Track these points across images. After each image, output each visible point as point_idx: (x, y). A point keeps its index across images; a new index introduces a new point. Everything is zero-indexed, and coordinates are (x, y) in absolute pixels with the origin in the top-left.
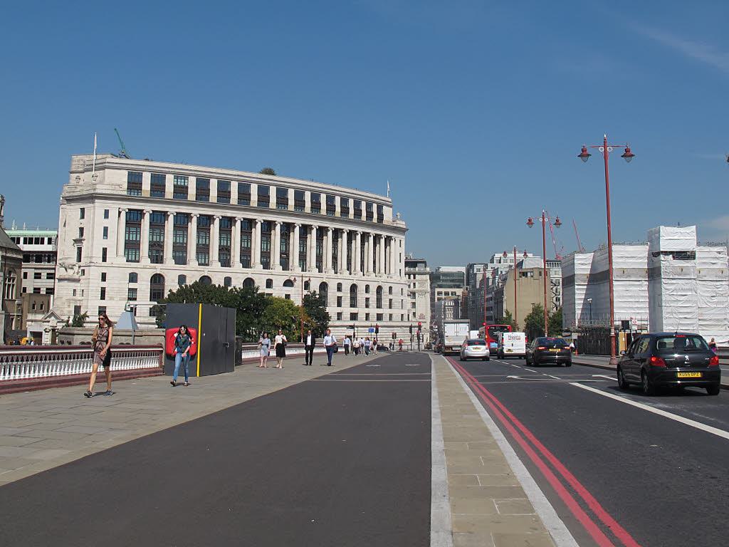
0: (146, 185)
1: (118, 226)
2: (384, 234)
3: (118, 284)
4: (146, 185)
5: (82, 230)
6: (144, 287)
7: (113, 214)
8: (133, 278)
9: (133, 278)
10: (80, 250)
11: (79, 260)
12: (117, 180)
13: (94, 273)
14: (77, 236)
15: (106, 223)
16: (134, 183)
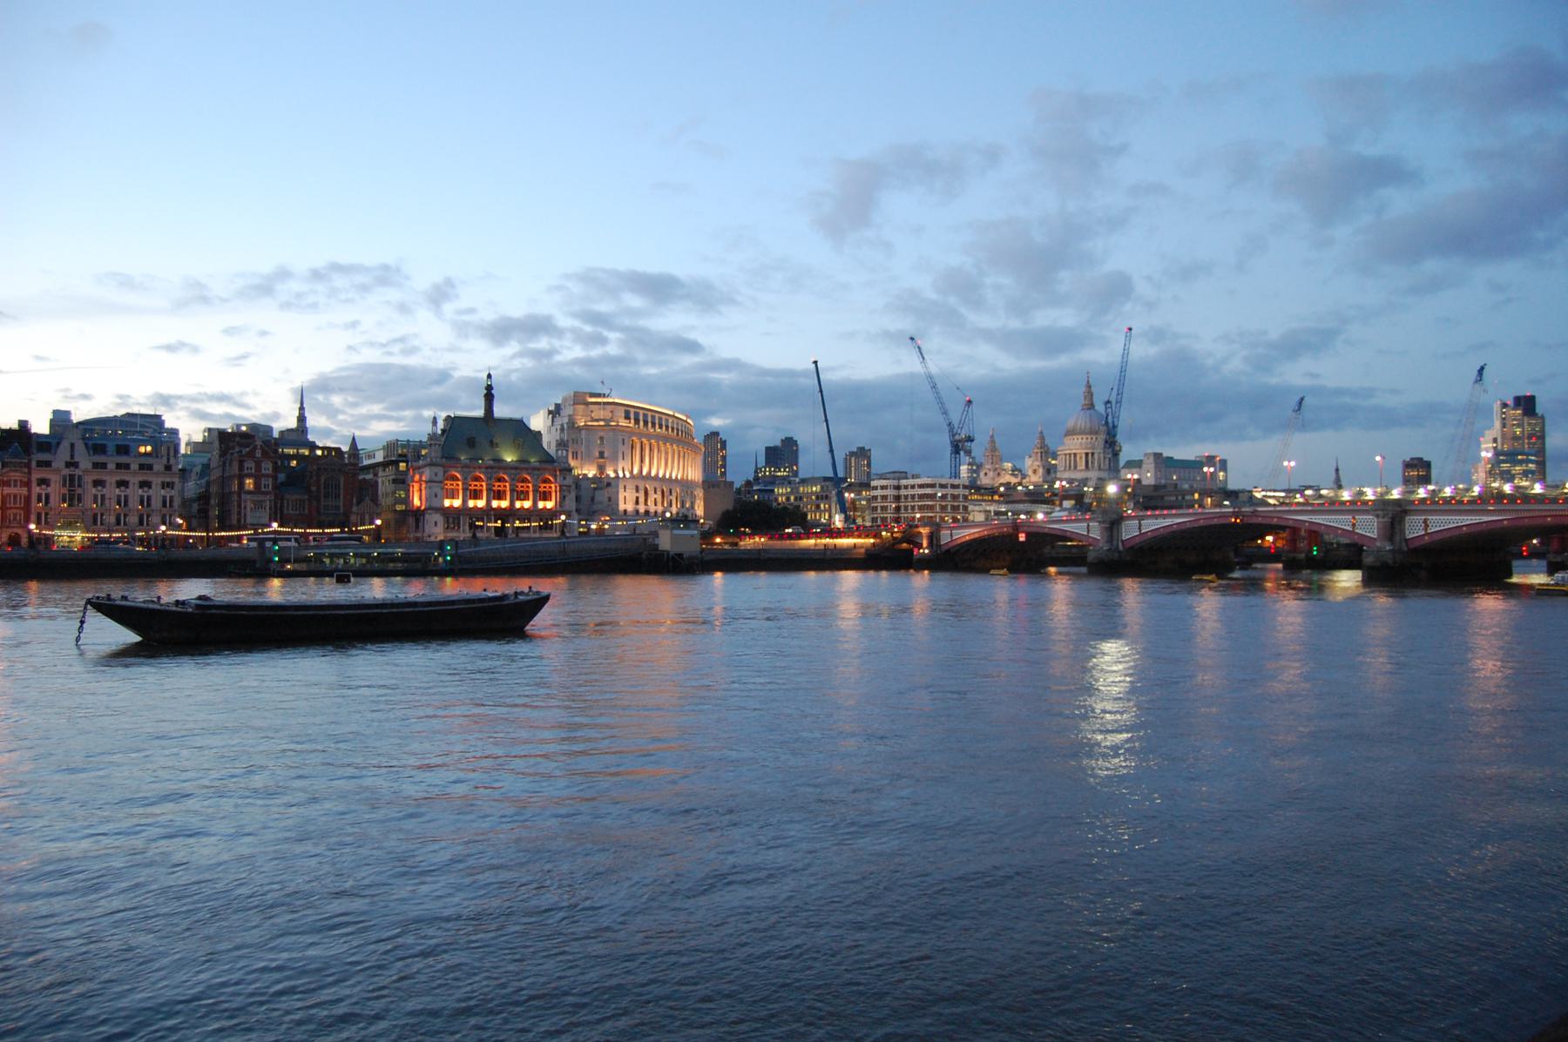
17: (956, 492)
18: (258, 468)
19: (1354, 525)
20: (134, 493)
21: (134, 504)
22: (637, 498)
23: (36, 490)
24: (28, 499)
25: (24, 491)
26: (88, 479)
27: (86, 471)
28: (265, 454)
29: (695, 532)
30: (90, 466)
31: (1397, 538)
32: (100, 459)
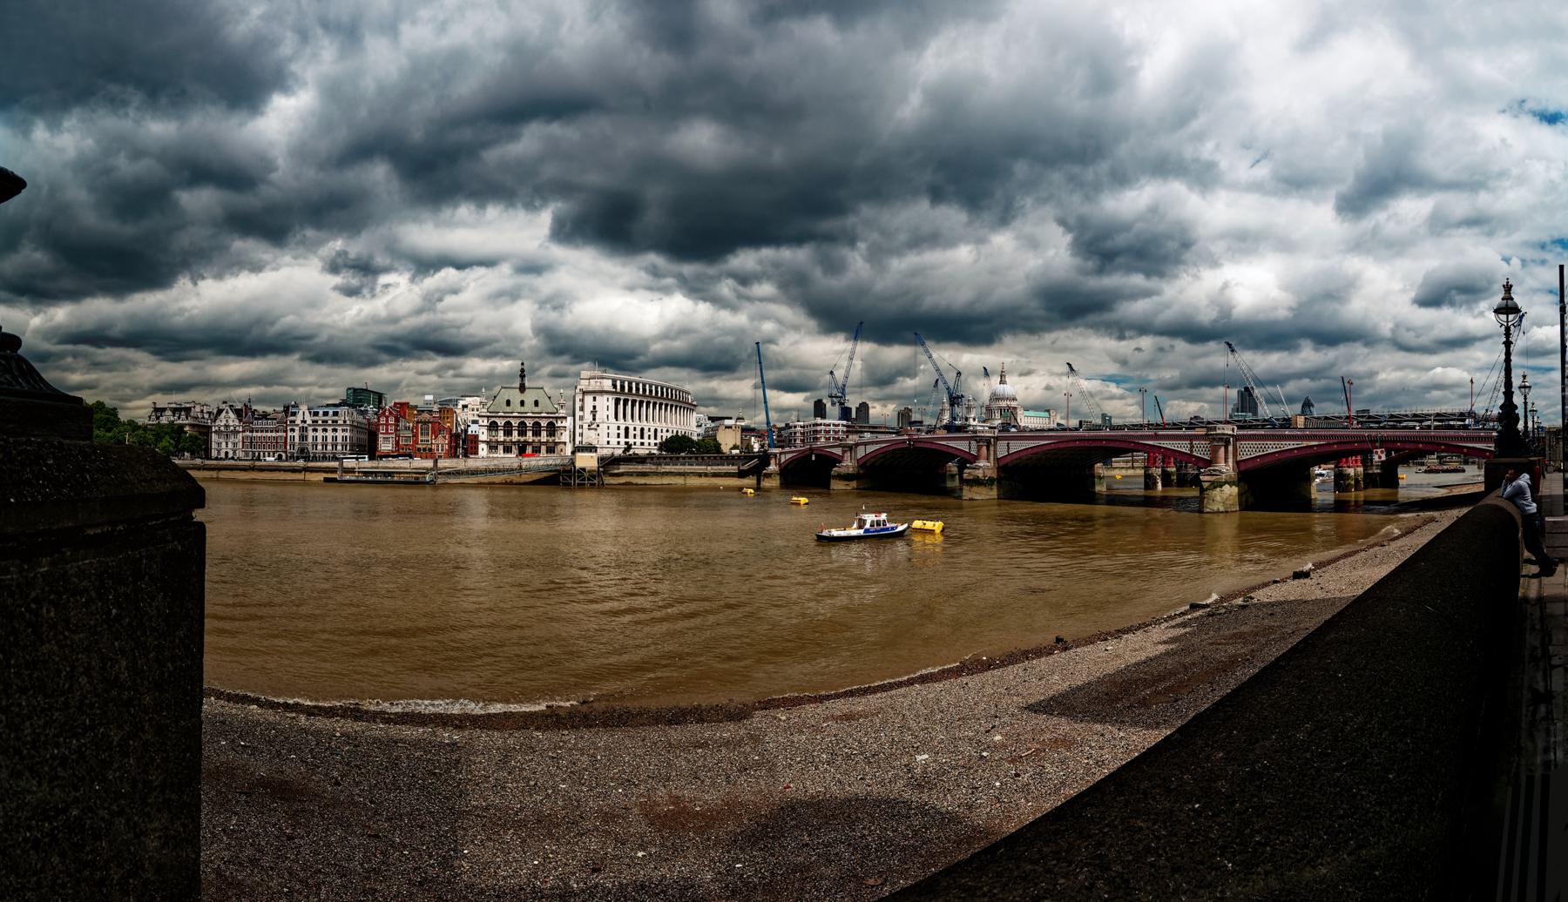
0: (619, 387)
1: (612, 404)
2: (692, 407)
3: (614, 431)
4: (619, 387)
5: (594, 407)
6: (622, 432)
7: (610, 399)
8: (619, 428)
9: (619, 428)
10: (594, 416)
11: (594, 419)
12: (607, 385)
13: (603, 427)
14: (592, 409)
15: (608, 404)
16: (615, 386)
17: (837, 429)
18: (387, 421)
19: (970, 448)
20: (330, 434)
21: (320, 440)
22: (619, 435)
23: (289, 434)
24: (286, 438)
25: (284, 434)
26: (310, 428)
27: (309, 425)
28: (390, 413)
29: (594, 454)
30: (311, 423)
31: (992, 458)
32: (316, 418)
